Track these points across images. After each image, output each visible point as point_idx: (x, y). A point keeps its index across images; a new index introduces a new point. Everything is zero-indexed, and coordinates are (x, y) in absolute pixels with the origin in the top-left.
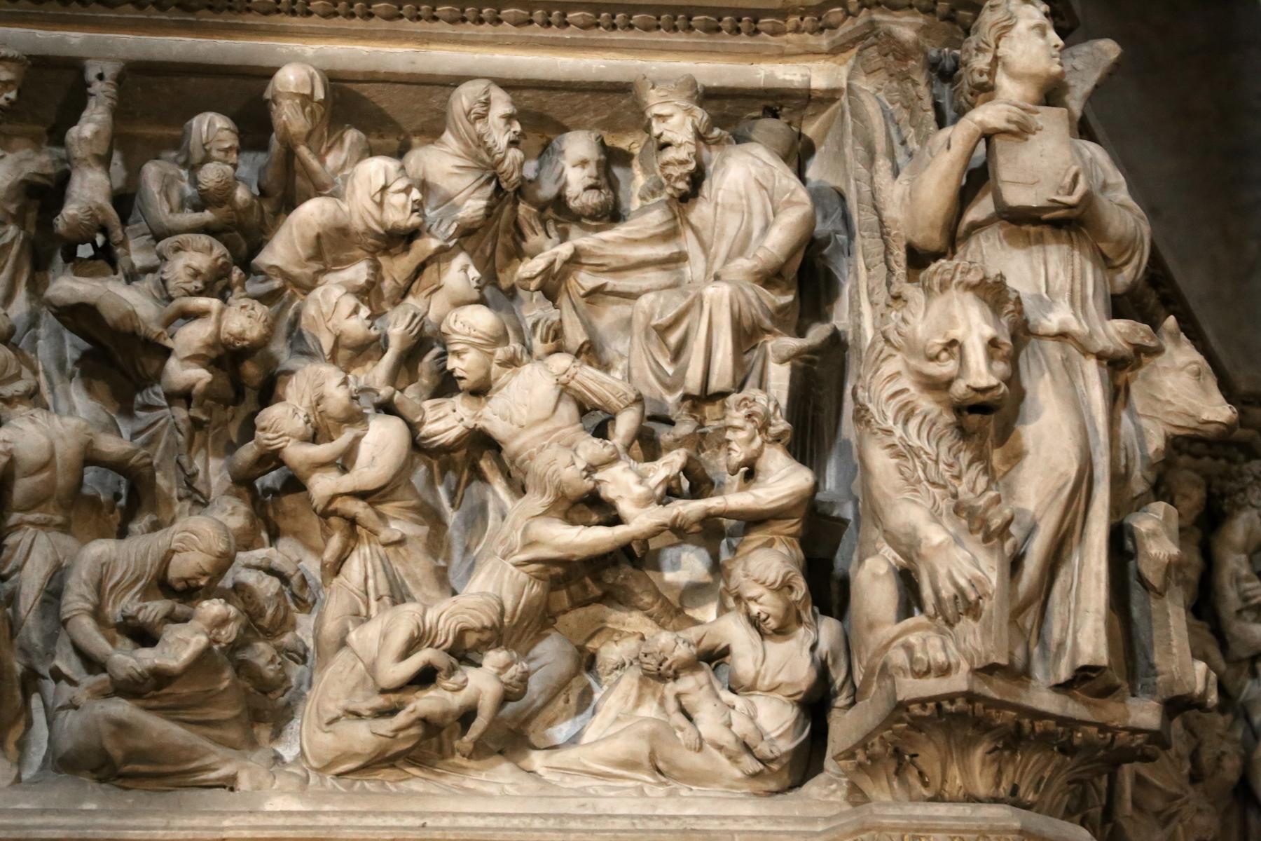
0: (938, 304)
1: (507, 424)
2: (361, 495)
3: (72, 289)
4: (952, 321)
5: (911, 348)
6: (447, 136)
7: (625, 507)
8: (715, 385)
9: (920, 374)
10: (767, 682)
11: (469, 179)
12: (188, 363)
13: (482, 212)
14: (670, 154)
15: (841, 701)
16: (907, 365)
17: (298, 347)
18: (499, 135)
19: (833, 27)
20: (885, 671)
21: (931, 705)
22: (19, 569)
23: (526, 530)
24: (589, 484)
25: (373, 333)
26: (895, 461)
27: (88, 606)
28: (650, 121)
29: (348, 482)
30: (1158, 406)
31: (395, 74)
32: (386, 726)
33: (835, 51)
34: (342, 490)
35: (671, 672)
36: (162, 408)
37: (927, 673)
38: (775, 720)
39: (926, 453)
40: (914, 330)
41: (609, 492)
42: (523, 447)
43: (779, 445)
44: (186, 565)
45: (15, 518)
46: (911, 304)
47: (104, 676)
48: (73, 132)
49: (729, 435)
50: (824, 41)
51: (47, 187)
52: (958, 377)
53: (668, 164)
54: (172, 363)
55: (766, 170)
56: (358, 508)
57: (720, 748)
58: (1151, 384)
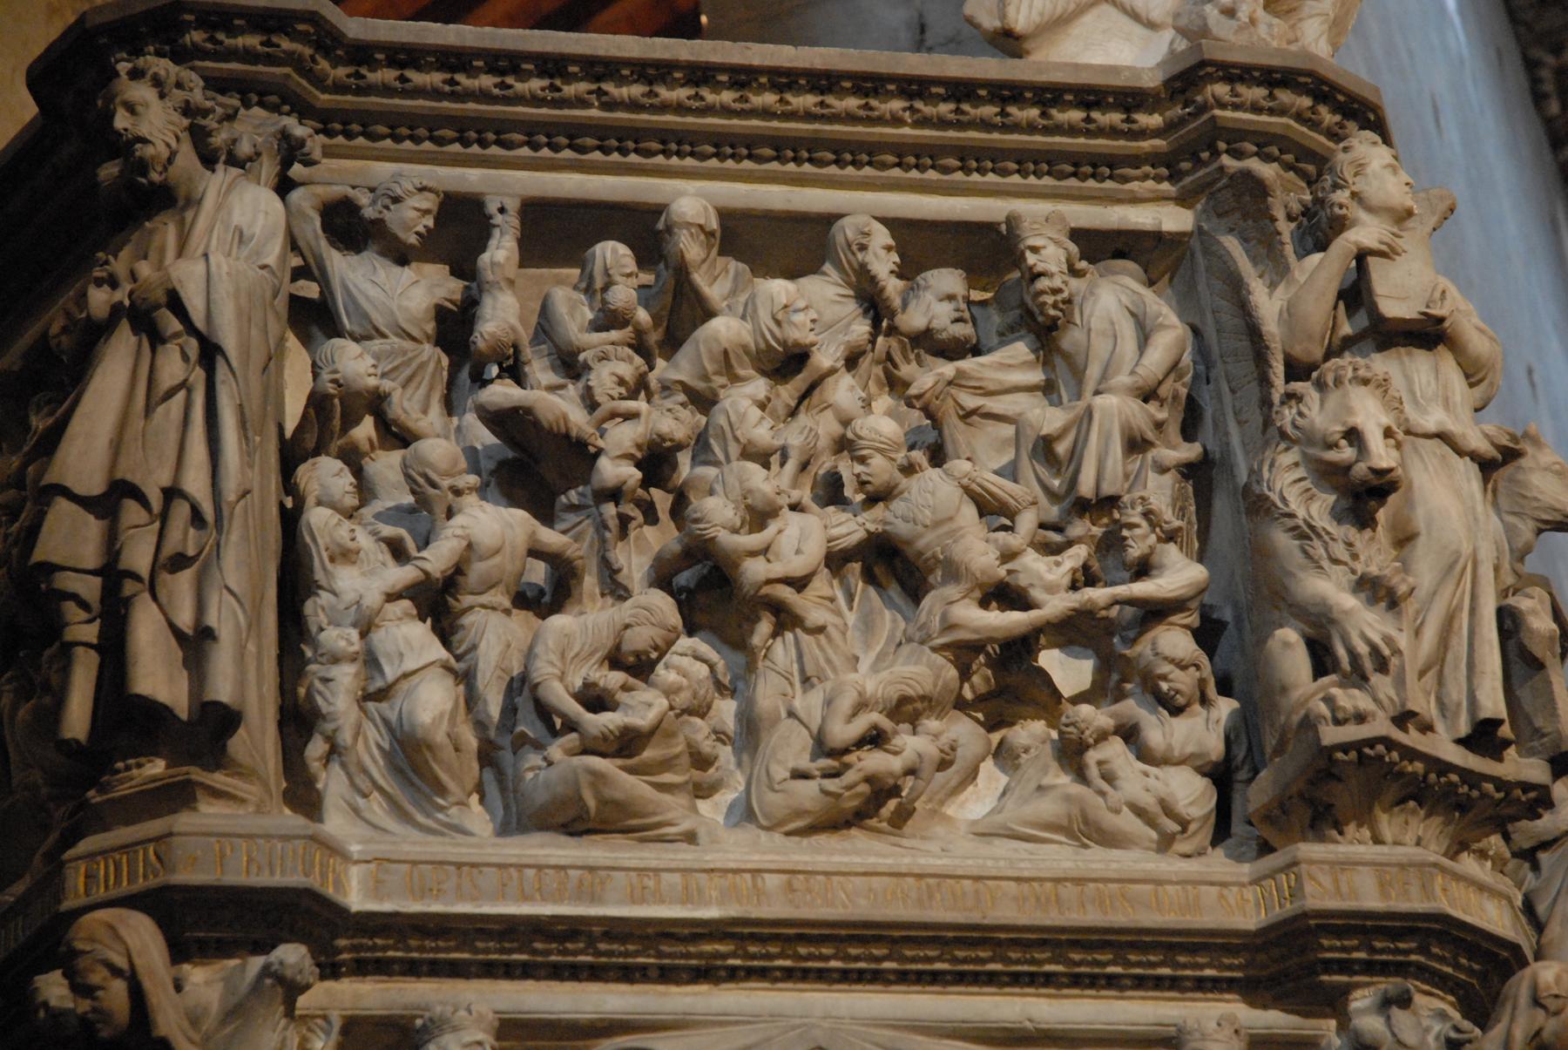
0: (1334, 398)
1: (910, 526)
2: (788, 581)
3: (505, 394)
4: (1349, 410)
6: (827, 267)
7: (1037, 594)
8: (1108, 489)
9: (1320, 461)
11: (852, 307)
12: (618, 461)
13: (867, 336)
14: (1043, 284)
15: (1242, 775)
16: (1304, 454)
17: (702, 457)
18: (883, 264)
20: (1309, 724)
22: (474, 647)
23: (944, 617)
24: (1002, 572)
25: (778, 443)
26: (1297, 542)
27: (556, 671)
28: (1023, 253)
29: (778, 569)
30: (1524, 502)
31: (771, 211)
32: (832, 785)
34: (772, 576)
35: (1091, 741)
36: (588, 507)
38: (1191, 793)
39: (1328, 533)
40: (1312, 421)
41: (1023, 581)
42: (928, 546)
44: (640, 638)
45: (467, 600)
46: (1307, 399)
47: (574, 735)
48: (485, 258)
49: (1125, 533)
51: (450, 311)
52: (1357, 461)
53: (1042, 292)
54: (604, 463)
55: (1135, 297)
56: (786, 593)
57: (1140, 812)
58: (1518, 482)
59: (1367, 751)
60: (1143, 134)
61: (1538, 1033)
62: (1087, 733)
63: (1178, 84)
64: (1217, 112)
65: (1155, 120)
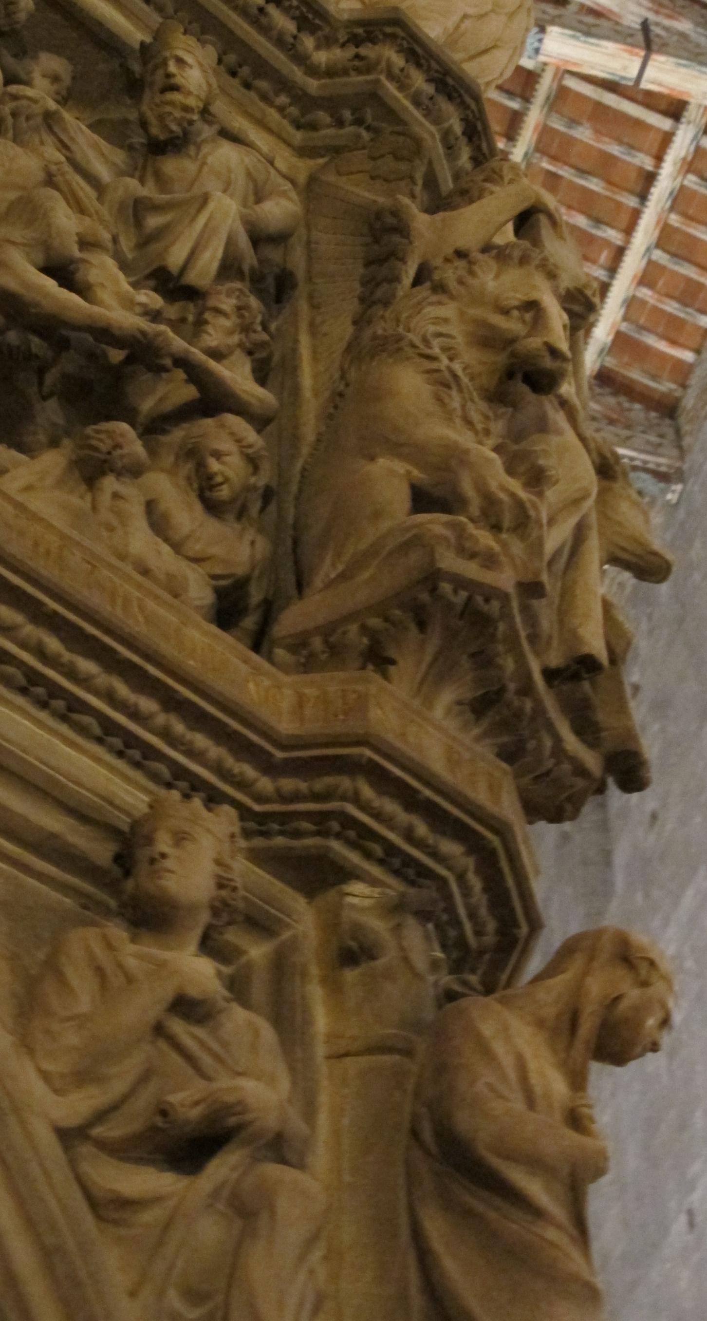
5: (478, 299)
7: (105, 295)
8: (192, 278)
10: (198, 547)
14: (176, 97)
16: (462, 313)
19: (313, 127)
21: (464, 594)
24: (76, 253)
33: (303, 152)
35: (119, 464)
37: (473, 556)
43: (249, 358)
50: (298, 137)
52: (528, 335)
53: (172, 103)
59: (479, 599)
60: (301, 59)
61: (617, 999)
62: (119, 452)
63: (360, 31)
64: (383, 78)
65: (322, 57)
